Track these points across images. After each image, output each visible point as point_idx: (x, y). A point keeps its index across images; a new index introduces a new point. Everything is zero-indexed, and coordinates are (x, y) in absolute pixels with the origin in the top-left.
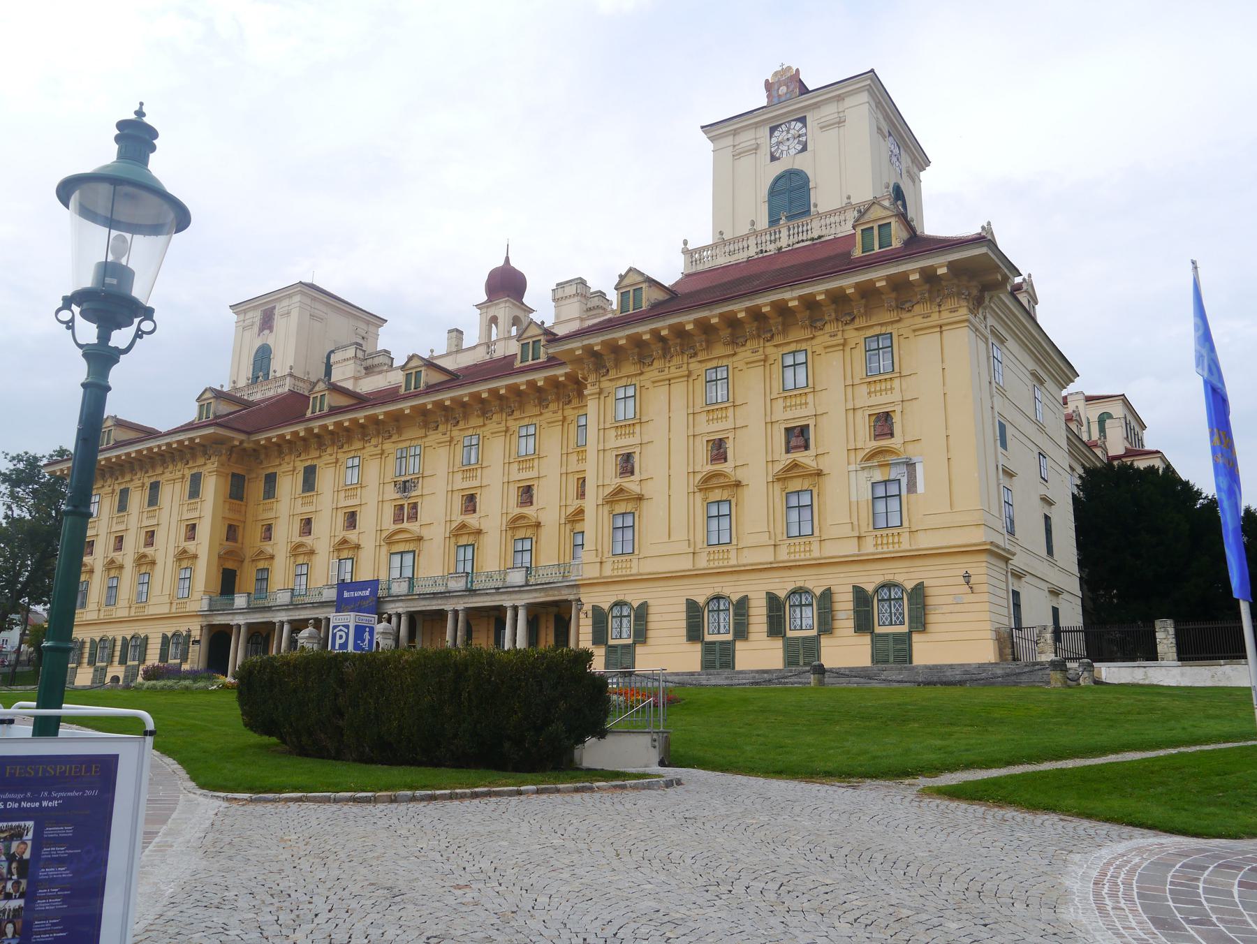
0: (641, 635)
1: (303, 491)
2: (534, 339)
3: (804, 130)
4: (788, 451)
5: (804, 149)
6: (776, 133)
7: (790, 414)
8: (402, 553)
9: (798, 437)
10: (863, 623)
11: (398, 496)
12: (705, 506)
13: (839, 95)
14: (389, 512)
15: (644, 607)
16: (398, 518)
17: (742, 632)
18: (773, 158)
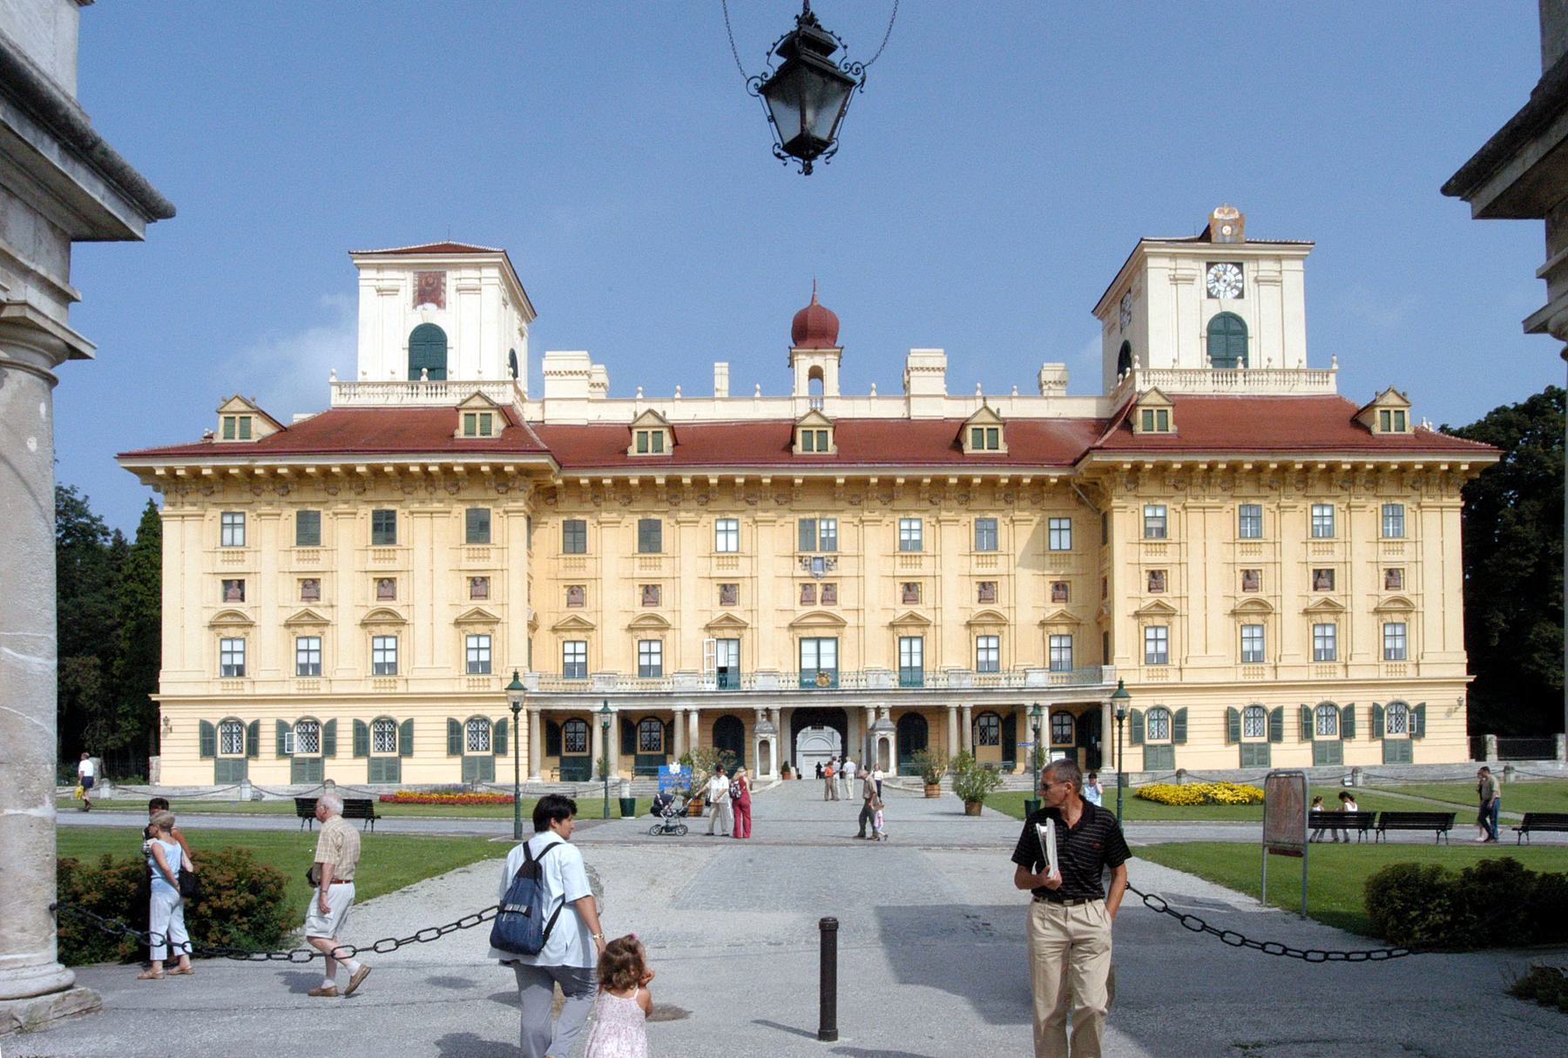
2: (990, 427)
3: (1240, 277)
5: (1241, 295)
6: (1212, 270)
8: (818, 640)
11: (806, 573)
12: (1311, 628)
13: (1278, 255)
14: (790, 594)
16: (807, 599)
18: (1210, 296)
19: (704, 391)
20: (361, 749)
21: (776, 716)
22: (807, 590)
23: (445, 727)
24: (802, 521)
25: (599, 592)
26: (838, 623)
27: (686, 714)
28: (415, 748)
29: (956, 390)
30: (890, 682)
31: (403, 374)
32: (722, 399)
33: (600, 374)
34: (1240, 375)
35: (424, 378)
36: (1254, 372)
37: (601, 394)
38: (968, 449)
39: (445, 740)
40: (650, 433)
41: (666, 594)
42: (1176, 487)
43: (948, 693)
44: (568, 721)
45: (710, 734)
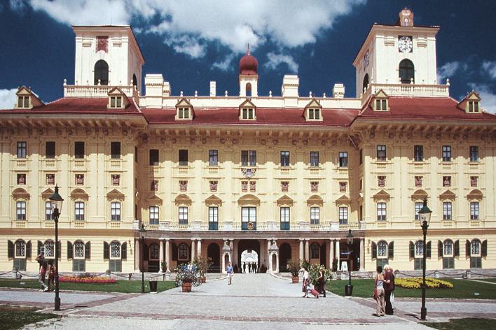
4: (444, 185)
5: (411, 51)
7: (445, 171)
11: (244, 177)
18: (400, 51)
19: (205, 92)
20: (70, 255)
21: (231, 243)
23: (103, 245)
27: (196, 242)
28: (91, 255)
29: (303, 93)
30: (277, 228)
31: (92, 83)
32: (213, 98)
33: (167, 87)
34: (412, 88)
35: (99, 84)
36: (417, 86)
37: (167, 95)
38: (308, 119)
42: (389, 137)
43: (300, 233)
44: (152, 244)
45: (206, 251)
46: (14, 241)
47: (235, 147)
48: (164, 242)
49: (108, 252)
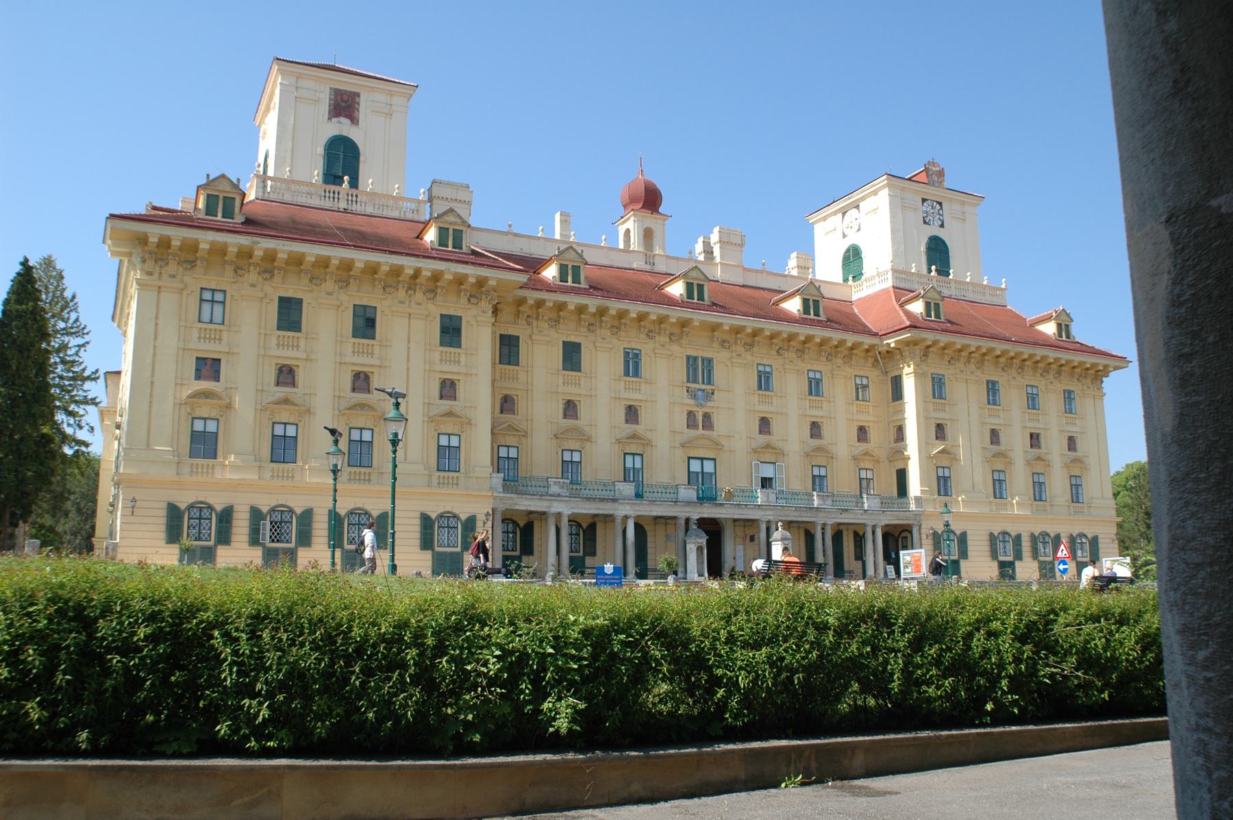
0: (964, 554)
1: (564, 369)
8: (702, 459)
9: (1035, 439)
10: (1035, 554)
14: (681, 420)
15: (964, 534)
17: (1018, 556)
22: (691, 414)
23: (418, 521)
24: (688, 357)
25: (530, 403)
26: (717, 446)
39: (418, 535)
40: (570, 267)
41: (583, 410)
46: (183, 506)
47: (675, 348)
48: (559, 515)
49: (432, 534)
